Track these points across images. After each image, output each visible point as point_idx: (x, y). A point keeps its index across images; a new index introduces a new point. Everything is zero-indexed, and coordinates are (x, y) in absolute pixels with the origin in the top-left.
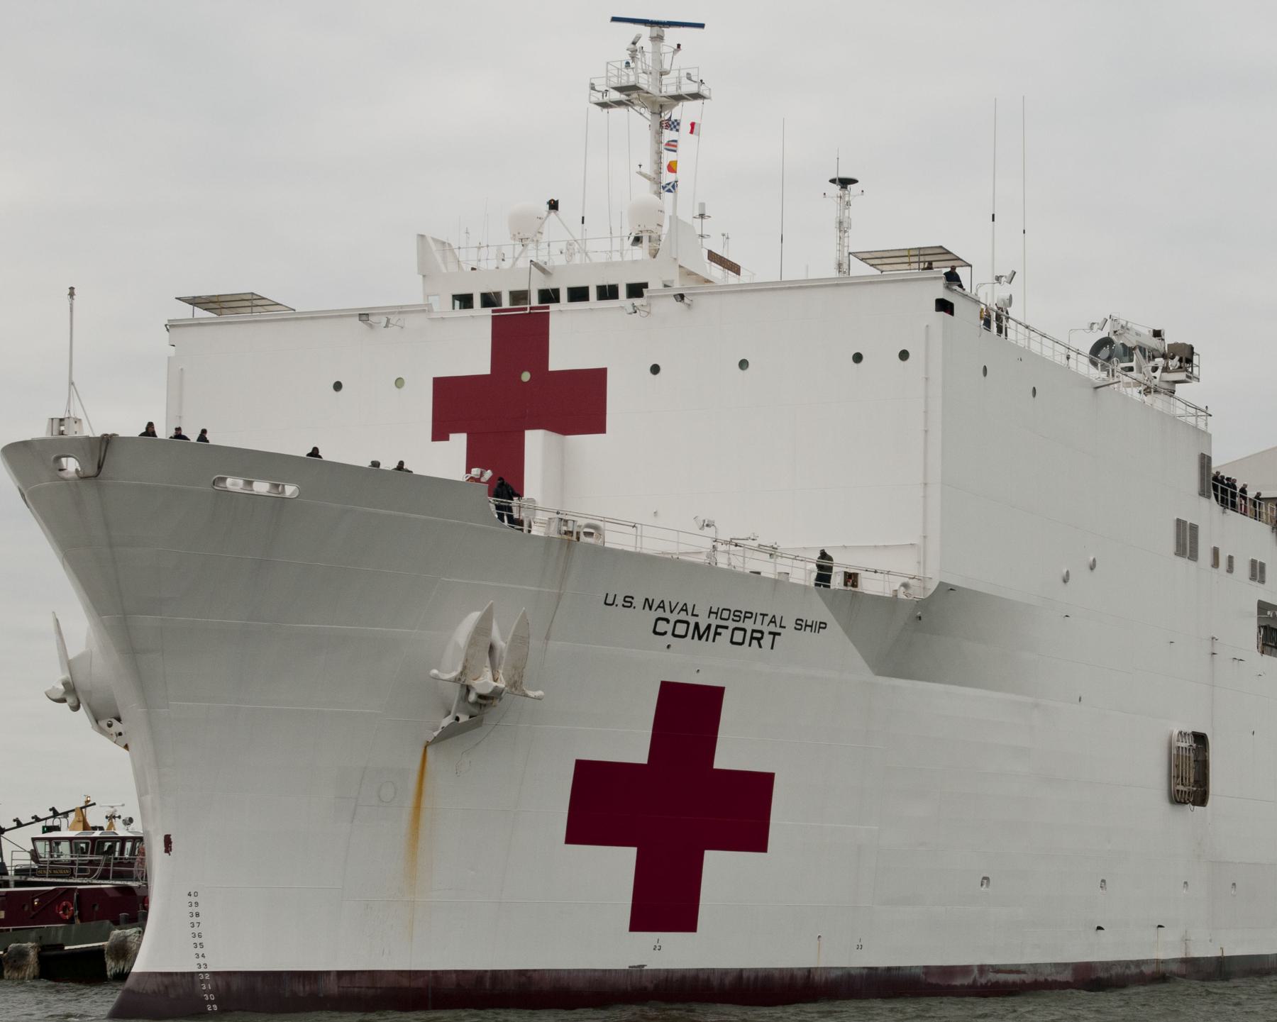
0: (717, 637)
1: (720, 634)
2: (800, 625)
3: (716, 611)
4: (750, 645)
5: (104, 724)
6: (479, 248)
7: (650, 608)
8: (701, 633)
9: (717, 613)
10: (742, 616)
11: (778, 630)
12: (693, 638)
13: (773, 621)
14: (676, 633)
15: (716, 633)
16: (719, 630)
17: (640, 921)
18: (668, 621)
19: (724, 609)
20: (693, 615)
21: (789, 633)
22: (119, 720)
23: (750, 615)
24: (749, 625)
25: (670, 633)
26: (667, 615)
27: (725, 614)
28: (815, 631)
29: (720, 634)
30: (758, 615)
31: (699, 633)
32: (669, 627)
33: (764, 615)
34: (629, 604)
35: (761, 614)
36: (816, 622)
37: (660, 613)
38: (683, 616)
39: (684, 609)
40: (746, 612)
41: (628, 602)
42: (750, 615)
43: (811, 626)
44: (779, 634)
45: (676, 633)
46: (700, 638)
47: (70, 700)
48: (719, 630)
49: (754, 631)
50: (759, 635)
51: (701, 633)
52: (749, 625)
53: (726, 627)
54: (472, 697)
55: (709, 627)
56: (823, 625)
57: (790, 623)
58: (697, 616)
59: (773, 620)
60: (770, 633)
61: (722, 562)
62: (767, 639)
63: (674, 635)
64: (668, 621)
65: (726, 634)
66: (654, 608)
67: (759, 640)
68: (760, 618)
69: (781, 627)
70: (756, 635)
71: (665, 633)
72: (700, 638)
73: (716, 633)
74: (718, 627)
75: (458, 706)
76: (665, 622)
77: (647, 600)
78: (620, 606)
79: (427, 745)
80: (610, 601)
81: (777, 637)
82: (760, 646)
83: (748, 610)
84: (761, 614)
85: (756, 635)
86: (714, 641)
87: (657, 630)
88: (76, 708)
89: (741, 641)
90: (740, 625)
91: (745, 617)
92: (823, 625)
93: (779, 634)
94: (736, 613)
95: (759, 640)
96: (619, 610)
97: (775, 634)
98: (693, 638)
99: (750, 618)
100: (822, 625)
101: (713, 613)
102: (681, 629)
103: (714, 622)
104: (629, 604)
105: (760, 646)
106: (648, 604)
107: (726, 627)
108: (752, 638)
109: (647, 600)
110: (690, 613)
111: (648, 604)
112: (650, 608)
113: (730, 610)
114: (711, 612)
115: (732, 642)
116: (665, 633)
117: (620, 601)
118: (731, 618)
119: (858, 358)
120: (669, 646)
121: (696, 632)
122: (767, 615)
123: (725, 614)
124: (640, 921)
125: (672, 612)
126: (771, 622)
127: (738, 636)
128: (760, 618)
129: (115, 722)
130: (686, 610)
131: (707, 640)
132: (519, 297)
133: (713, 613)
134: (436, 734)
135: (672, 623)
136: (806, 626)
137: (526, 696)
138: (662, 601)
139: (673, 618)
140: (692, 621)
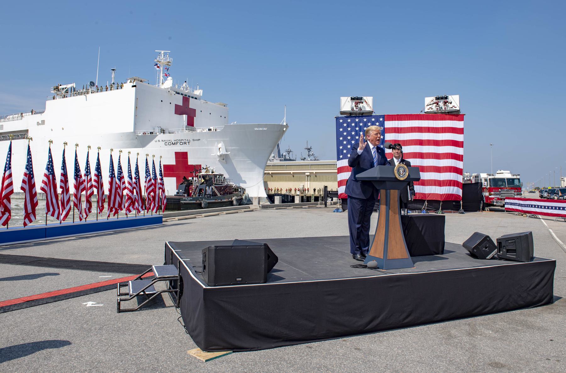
2: (194, 140)
11: (189, 141)
13: (187, 140)
21: (192, 142)
24: (183, 141)
37: (165, 142)
38: (169, 142)
41: (159, 141)
55: (175, 143)
57: (191, 140)
62: (187, 143)
90: (181, 142)
96: (158, 142)
102: (170, 144)
106: (163, 141)
111: (163, 141)
117: (157, 141)
123: (177, 140)
127: (181, 143)
135: (168, 143)
139: (168, 142)
140: (172, 142)
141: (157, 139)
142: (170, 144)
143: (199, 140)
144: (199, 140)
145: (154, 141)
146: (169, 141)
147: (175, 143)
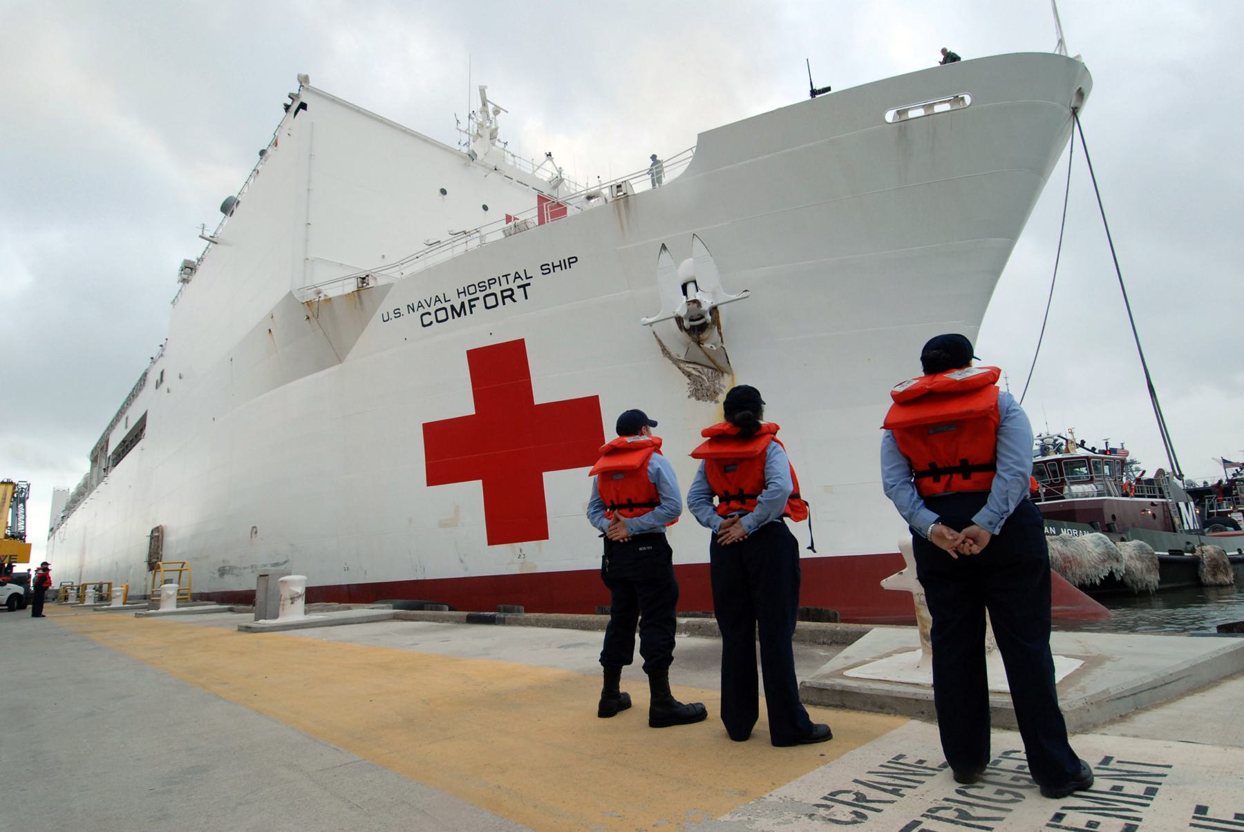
0: (473, 309)
1: (474, 306)
2: (546, 269)
3: (463, 291)
4: (504, 304)
7: (414, 310)
8: (458, 311)
9: (464, 292)
10: (487, 284)
12: (454, 318)
13: (517, 276)
14: (439, 319)
15: (471, 307)
16: (472, 303)
18: (429, 314)
20: (446, 301)
21: (538, 281)
24: (496, 289)
25: (434, 321)
26: (427, 309)
27: (472, 290)
28: (566, 268)
29: (474, 306)
30: (501, 278)
31: (458, 312)
32: (432, 318)
33: (506, 276)
35: (503, 276)
36: (564, 260)
38: (439, 305)
39: (438, 300)
40: (489, 281)
41: (398, 313)
42: (493, 281)
43: (560, 265)
44: (529, 284)
45: (439, 319)
46: (459, 315)
48: (472, 303)
49: (502, 292)
50: (509, 293)
51: (459, 311)
52: (496, 289)
53: (478, 299)
55: (463, 305)
57: (535, 271)
58: (449, 300)
59: (517, 276)
60: (519, 287)
62: (519, 294)
63: (438, 321)
64: (429, 314)
65: (479, 304)
66: (416, 309)
67: (511, 296)
68: (503, 280)
69: (527, 278)
70: (505, 294)
71: (431, 323)
72: (459, 315)
74: (470, 301)
77: (408, 306)
78: (393, 318)
80: (386, 319)
81: (527, 288)
82: (514, 301)
83: (490, 278)
84: (503, 276)
85: (505, 294)
86: (471, 313)
87: (425, 323)
89: (495, 304)
91: (489, 284)
93: (529, 284)
94: (481, 285)
95: (511, 296)
96: (394, 322)
97: (524, 286)
98: (454, 318)
99: (494, 283)
100: (571, 261)
101: (462, 293)
102: (442, 315)
103: (465, 299)
104: (399, 315)
105: (514, 301)
106: (411, 308)
107: (478, 299)
108: (503, 298)
109: (408, 306)
110: (443, 300)
111: (411, 308)
112: (414, 310)
113: (473, 285)
114: (459, 294)
115: (487, 308)
116: (431, 323)
117: (392, 315)
118: (478, 290)
121: (454, 312)
122: (509, 275)
123: (472, 290)
125: (429, 306)
126: (516, 278)
127: (491, 301)
128: (503, 280)
130: (439, 300)
131: (465, 314)
133: (462, 293)
135: (433, 314)
136: (554, 267)
138: (420, 302)
139: (432, 310)
140: (448, 306)
141: (387, 306)
142: (442, 315)
143: (573, 260)
144: (573, 260)
145: (377, 317)
146: (438, 300)
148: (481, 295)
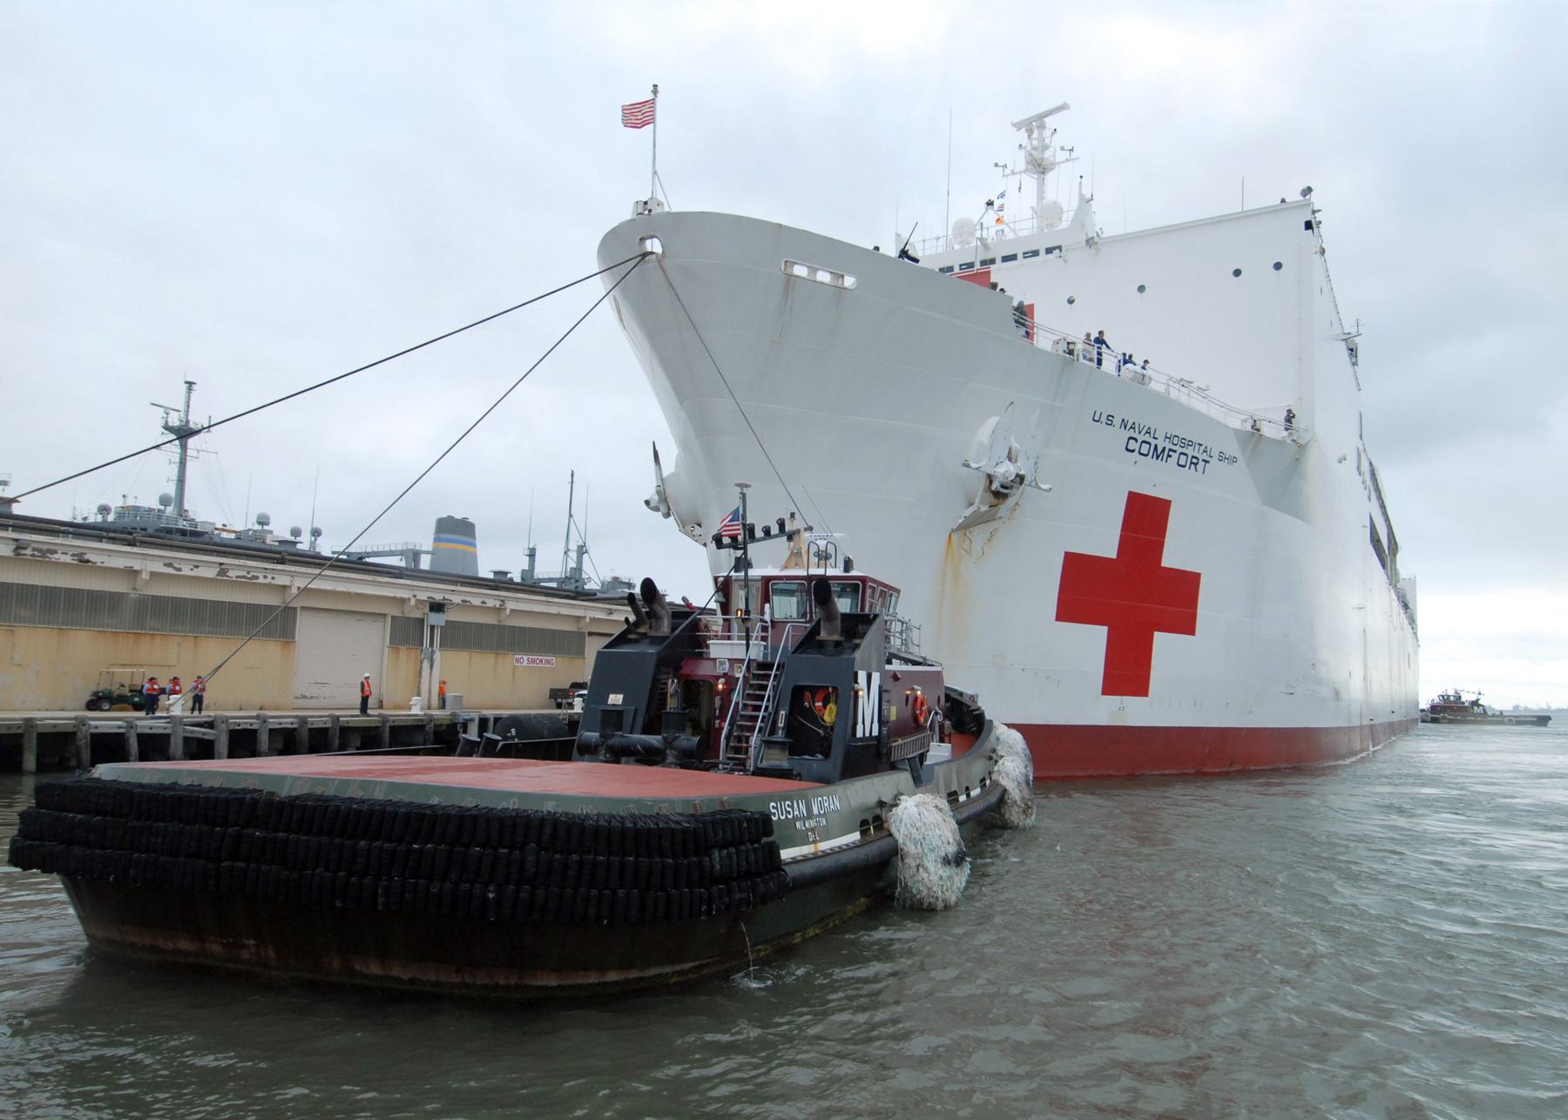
0: (1169, 458)
1: (1170, 456)
2: (1222, 457)
5: (689, 528)
6: (938, 239)
7: (1125, 428)
8: (1159, 453)
11: (1208, 459)
12: (1152, 457)
16: (1171, 453)
17: (1113, 685)
18: (1136, 440)
19: (1146, 455)
22: (699, 525)
23: (1190, 443)
24: (1189, 451)
29: (1170, 456)
31: (1158, 454)
33: (1200, 445)
34: (1110, 422)
37: (1131, 433)
38: (1147, 438)
42: (1190, 443)
44: (1208, 462)
46: (1157, 458)
47: (663, 508)
49: (1193, 457)
51: (1159, 453)
52: (1189, 451)
53: (1175, 451)
54: (995, 486)
55: (1164, 449)
56: (1234, 460)
57: (1215, 454)
58: (1156, 438)
60: (1204, 460)
61: (1174, 394)
62: (1201, 464)
64: (1136, 440)
65: (1175, 456)
66: (1128, 428)
67: (1196, 464)
68: (1197, 446)
71: (1133, 451)
72: (1157, 458)
73: (1169, 456)
74: (1170, 450)
75: (981, 499)
76: (1134, 441)
77: (1123, 420)
78: (1104, 423)
79: (953, 531)
80: (1096, 418)
81: (1207, 464)
82: (1196, 470)
87: (1129, 447)
88: (667, 515)
90: (1183, 450)
92: (1234, 460)
93: (1208, 462)
98: (1152, 457)
102: (1145, 449)
103: (1169, 446)
104: (1110, 422)
105: (1196, 470)
107: (1175, 451)
108: (1192, 463)
109: (1123, 420)
111: (1124, 423)
112: (1125, 428)
114: (1166, 437)
116: (1133, 451)
117: (1104, 419)
119: (1237, 273)
120: (1136, 462)
124: (1113, 685)
125: (1140, 433)
127: (1183, 460)
129: (696, 526)
131: (1162, 460)
132: (971, 265)
134: (960, 521)
135: (1139, 443)
137: (1039, 488)
139: (1140, 438)
140: (1153, 442)
142: (1145, 449)
147: (1164, 449)
148: (1180, 450)
